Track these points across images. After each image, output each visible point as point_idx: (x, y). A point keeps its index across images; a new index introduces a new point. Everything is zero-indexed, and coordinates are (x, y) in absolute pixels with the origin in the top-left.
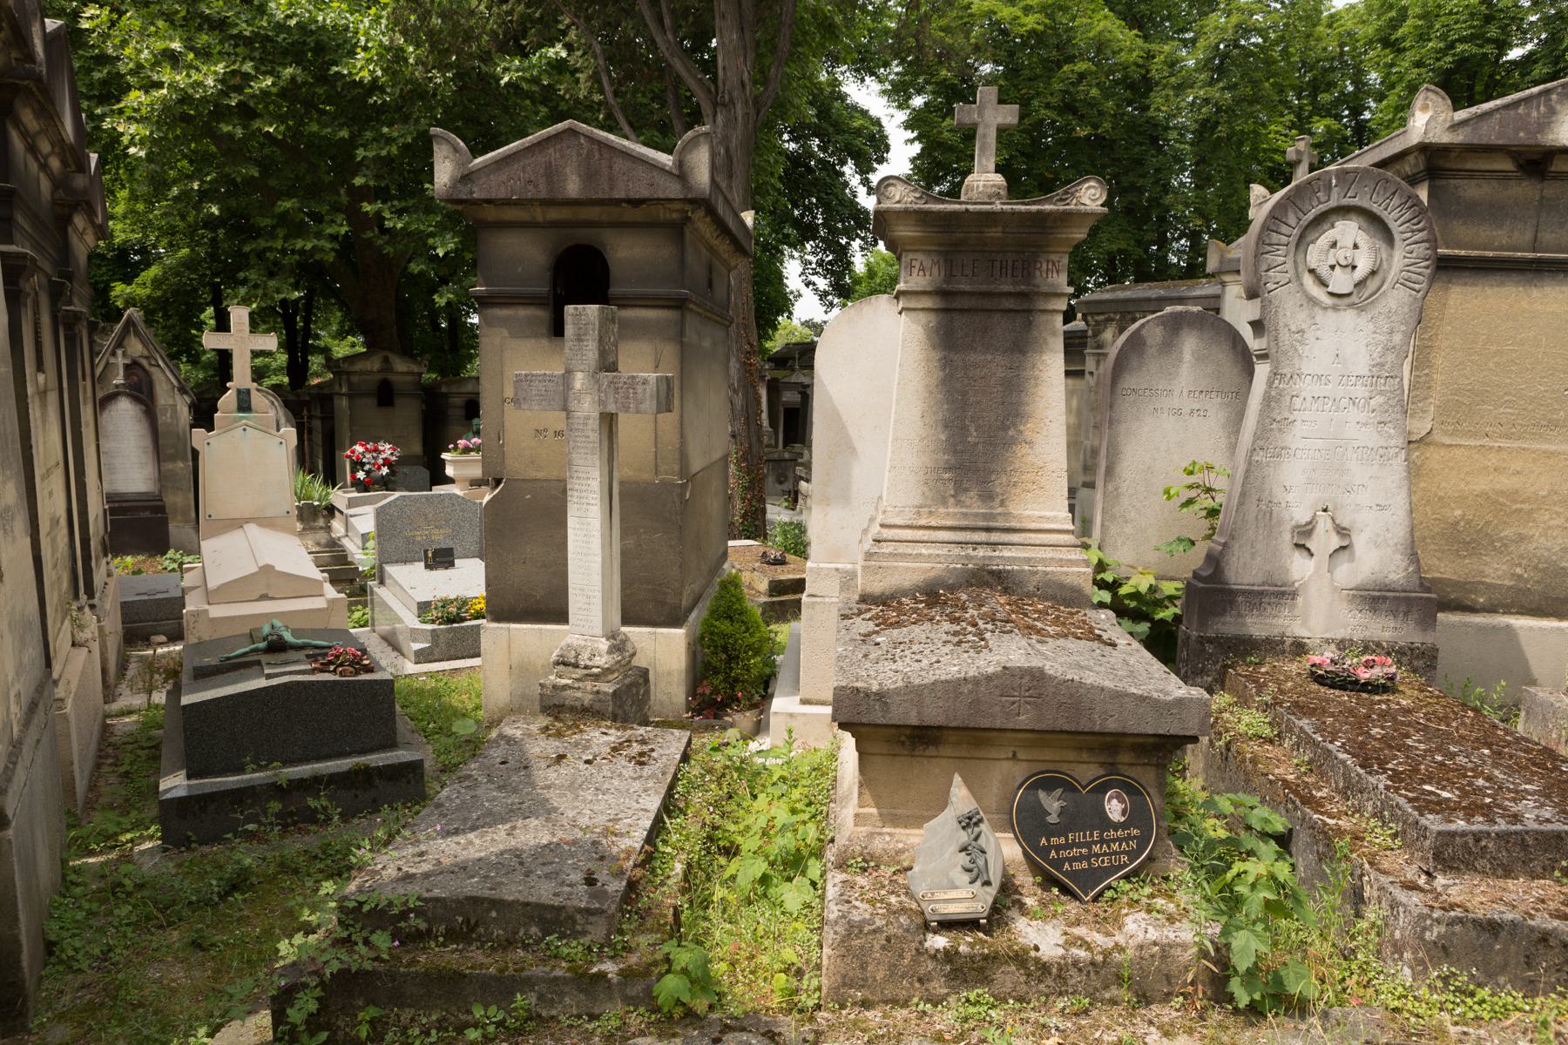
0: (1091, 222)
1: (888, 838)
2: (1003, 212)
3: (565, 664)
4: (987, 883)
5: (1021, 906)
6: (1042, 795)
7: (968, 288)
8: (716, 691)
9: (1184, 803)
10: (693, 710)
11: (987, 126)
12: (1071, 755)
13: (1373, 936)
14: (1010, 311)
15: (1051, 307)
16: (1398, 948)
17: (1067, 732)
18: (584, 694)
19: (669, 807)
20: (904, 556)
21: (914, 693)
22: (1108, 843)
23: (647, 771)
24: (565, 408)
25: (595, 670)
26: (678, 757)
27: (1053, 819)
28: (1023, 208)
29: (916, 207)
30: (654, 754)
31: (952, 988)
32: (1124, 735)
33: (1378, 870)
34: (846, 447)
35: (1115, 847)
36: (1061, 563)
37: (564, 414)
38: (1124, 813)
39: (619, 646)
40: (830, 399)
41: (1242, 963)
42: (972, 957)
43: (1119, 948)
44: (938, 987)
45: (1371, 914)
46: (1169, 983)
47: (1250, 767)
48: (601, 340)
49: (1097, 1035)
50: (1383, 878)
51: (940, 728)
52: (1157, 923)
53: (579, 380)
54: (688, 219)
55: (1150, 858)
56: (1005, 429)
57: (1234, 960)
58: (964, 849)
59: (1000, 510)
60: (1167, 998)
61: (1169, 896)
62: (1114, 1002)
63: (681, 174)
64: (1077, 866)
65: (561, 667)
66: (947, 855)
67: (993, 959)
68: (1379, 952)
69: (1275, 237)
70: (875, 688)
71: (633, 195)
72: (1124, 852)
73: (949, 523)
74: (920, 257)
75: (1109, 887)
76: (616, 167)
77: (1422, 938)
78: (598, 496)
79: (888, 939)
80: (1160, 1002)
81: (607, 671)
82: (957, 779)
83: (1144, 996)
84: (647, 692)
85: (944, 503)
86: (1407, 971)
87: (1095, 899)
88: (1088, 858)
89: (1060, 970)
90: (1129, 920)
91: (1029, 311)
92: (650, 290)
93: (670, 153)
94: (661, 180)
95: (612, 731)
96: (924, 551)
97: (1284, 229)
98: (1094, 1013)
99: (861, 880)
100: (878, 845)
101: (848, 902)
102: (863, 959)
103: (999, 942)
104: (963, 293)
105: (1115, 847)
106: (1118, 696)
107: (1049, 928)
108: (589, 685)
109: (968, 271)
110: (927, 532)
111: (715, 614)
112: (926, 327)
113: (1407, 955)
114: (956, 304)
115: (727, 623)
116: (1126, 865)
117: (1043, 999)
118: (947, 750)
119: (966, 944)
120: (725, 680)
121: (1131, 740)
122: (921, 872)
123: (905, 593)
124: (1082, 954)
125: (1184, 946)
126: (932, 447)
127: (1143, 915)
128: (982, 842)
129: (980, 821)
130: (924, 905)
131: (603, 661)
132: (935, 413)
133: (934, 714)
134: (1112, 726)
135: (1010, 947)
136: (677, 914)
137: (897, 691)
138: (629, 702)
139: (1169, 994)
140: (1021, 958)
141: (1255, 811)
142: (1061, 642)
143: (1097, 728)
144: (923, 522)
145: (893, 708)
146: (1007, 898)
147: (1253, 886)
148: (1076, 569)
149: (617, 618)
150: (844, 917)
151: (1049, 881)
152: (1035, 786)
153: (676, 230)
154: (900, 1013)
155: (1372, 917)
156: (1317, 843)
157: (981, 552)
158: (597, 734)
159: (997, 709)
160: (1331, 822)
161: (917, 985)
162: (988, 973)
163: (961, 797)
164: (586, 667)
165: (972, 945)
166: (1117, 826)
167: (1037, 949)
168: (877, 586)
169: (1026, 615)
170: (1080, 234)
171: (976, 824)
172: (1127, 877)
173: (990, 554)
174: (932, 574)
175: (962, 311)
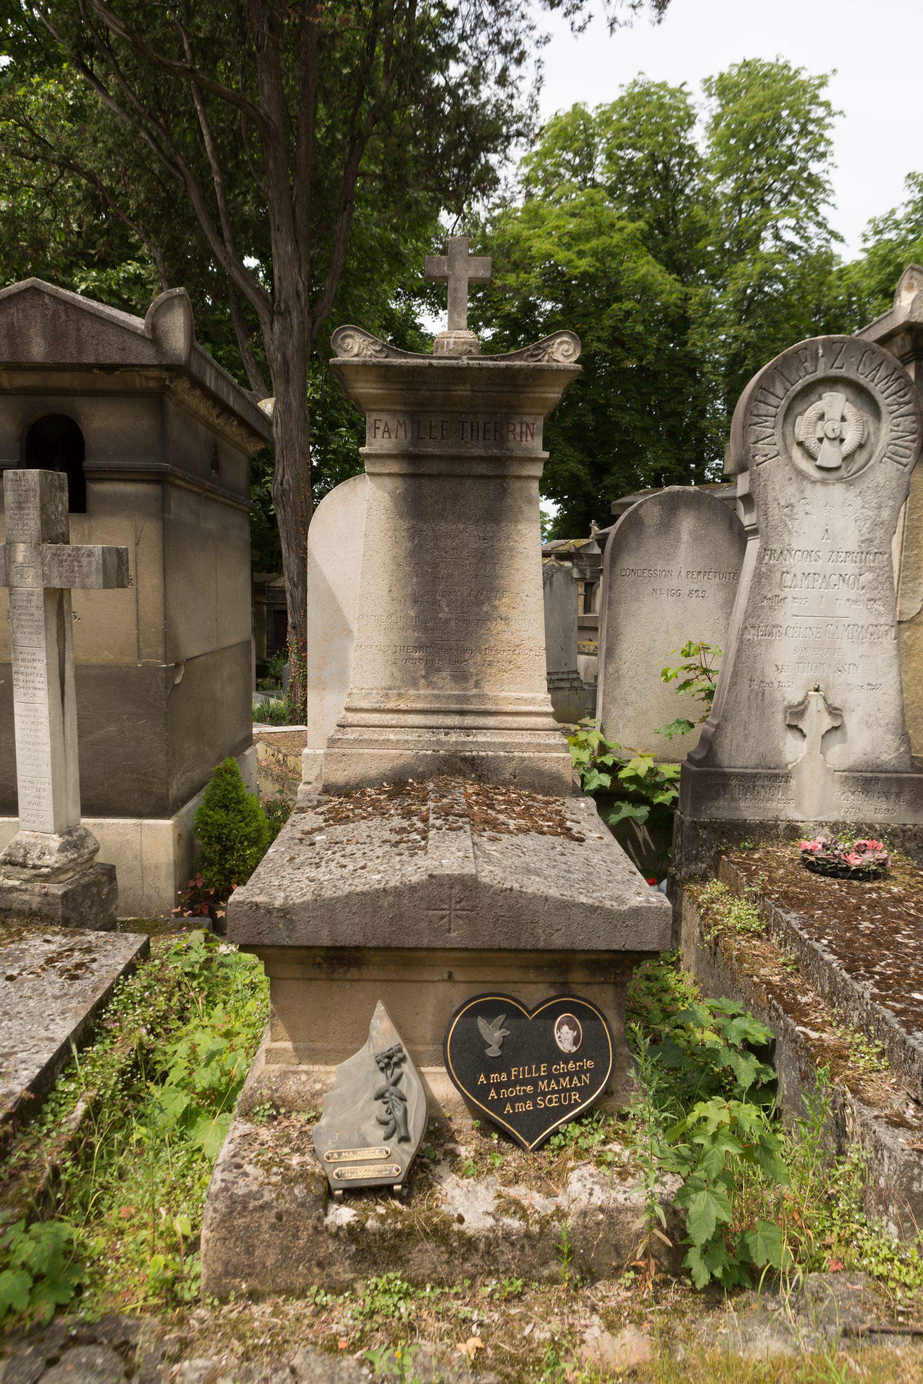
0: (565, 381)
1: (304, 1077)
2: (469, 368)
3: (13, 864)
4: (405, 1139)
5: (453, 1156)
6: (481, 1022)
7: (436, 451)
8: (208, 885)
9: (675, 1000)
10: (182, 905)
11: (457, 279)
12: (516, 975)
13: (855, 1180)
14: (483, 477)
15: (525, 473)
16: (883, 1200)
17: (505, 950)
18: (31, 897)
19: (87, 1034)
20: (371, 743)
21: (324, 907)
22: (557, 1078)
23: (77, 985)
24: (8, 584)
25: (45, 870)
26: (120, 968)
27: (493, 1051)
28: (490, 363)
29: (374, 360)
30: (94, 966)
31: (360, 1272)
32: (574, 951)
33: (862, 1100)
34: (340, 629)
35: (565, 1082)
36: (539, 747)
37: (7, 590)
38: (575, 1042)
39: (74, 840)
40: (324, 579)
41: (701, 1234)
42: (382, 1235)
43: (560, 1214)
44: (342, 1272)
45: (856, 1152)
46: (619, 1255)
47: (736, 966)
48: (43, 508)
49: (526, 1332)
50: (866, 1111)
51: (357, 948)
52: (601, 1182)
53: (21, 553)
54: (167, 388)
55: (608, 1093)
56: (480, 604)
57: (691, 1229)
58: (380, 1096)
59: (474, 691)
60: (617, 1272)
61: (626, 1141)
62: (554, 1280)
63: (155, 338)
64: (520, 1107)
65: (8, 868)
66: (360, 1104)
67: (407, 1235)
68: (862, 1200)
69: (763, 409)
70: (278, 903)
71: (103, 360)
72: (575, 1089)
73: (420, 706)
74: (385, 417)
75: (556, 1133)
76: (85, 330)
77: (909, 1190)
78: (44, 679)
79: (279, 1217)
80: (608, 1278)
81: (57, 871)
82: (380, 1008)
83: (589, 1271)
84: (114, 891)
85: (415, 685)
86: (893, 1228)
87: (540, 1147)
88: (533, 1097)
89: (489, 1244)
90: (573, 1177)
91: (504, 477)
92: (127, 463)
93: (140, 314)
94: (133, 344)
95: (58, 938)
96: (392, 737)
97: (772, 400)
98: (527, 1298)
99: (265, 1134)
100: (291, 1087)
101: (238, 1166)
102: (248, 1241)
103: (414, 1212)
104: (433, 457)
105: (565, 1082)
106: (565, 906)
107: (481, 1188)
108: (37, 886)
109: (437, 434)
110: (395, 716)
111: (210, 803)
112: (392, 495)
113: (893, 1209)
114: (424, 469)
115: (222, 812)
116: (577, 1104)
117: (467, 1283)
118: (371, 973)
119: (376, 1216)
120: (219, 872)
121: (582, 957)
122: (329, 1125)
123: (371, 783)
124: (514, 1224)
125: (635, 1212)
126: (401, 624)
127: (591, 1168)
128: (402, 1086)
129: (403, 1060)
130: (328, 1169)
131: (52, 860)
132: (404, 587)
133: (349, 934)
134: (559, 941)
135: (428, 1219)
136: (56, 1171)
137: (304, 906)
138: (88, 902)
139: (618, 1268)
140: (440, 1232)
141: (736, 1021)
142: (520, 839)
143: (541, 945)
144: (391, 705)
145: (300, 926)
146: (434, 1149)
147: (714, 1137)
148: (557, 754)
149: (74, 809)
150: (226, 1189)
151: (487, 1126)
152: (473, 1013)
153: (157, 400)
154: (294, 1307)
155: (855, 1157)
156: (799, 1059)
157: (453, 737)
158: (38, 942)
159: (424, 924)
160: (814, 1035)
161: (316, 1270)
162: (402, 1252)
163: (382, 1031)
164: (35, 867)
165: (382, 1218)
166: (567, 1058)
167: (461, 1220)
168: (341, 775)
169: (491, 806)
170: (554, 394)
171: (397, 1064)
172: (577, 1119)
173: (464, 739)
174: (400, 762)
175: (430, 476)
